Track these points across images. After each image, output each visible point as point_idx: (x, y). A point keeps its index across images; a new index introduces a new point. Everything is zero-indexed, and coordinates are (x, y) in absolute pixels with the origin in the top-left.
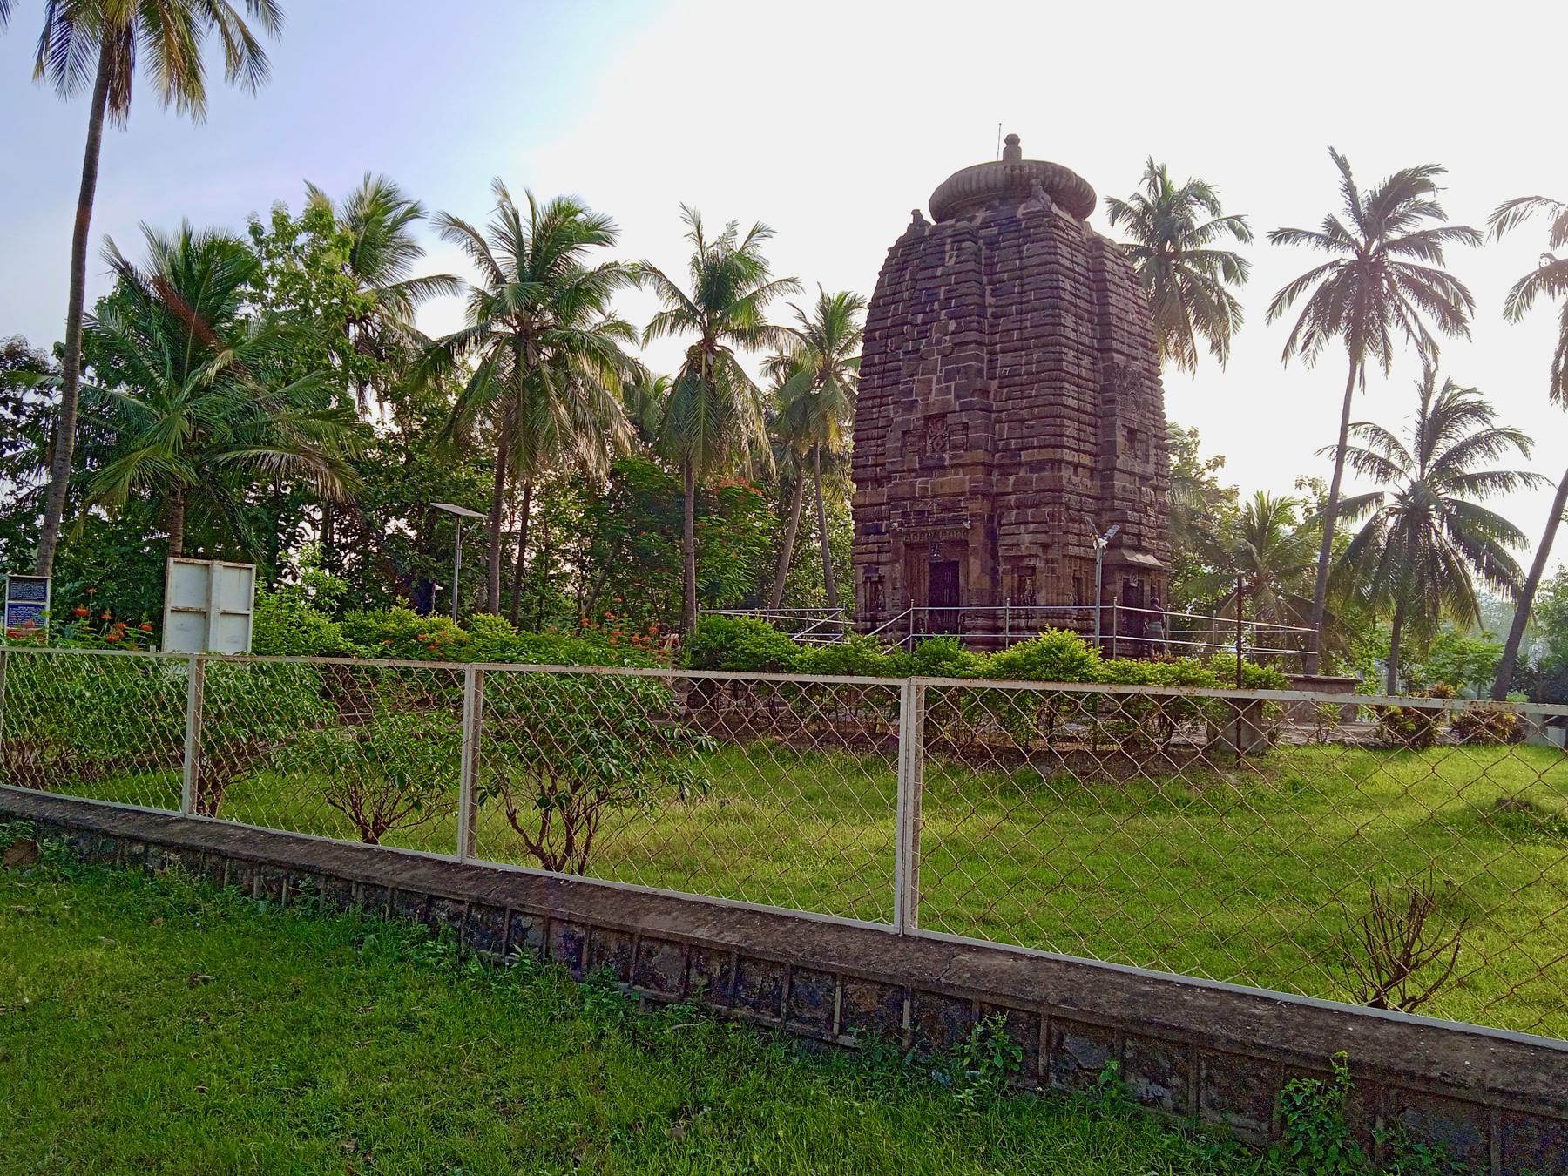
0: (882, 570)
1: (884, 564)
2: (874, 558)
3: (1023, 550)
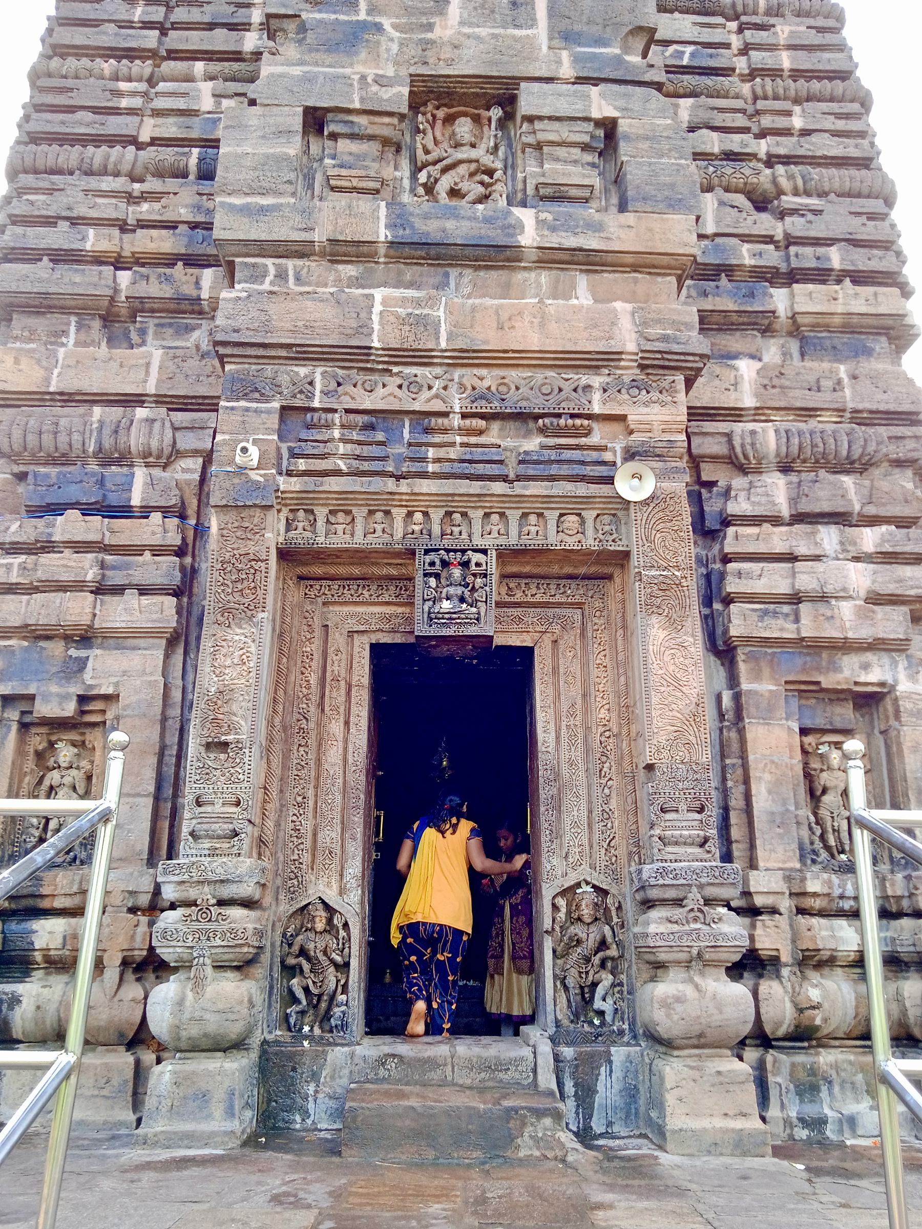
0: (103, 669)
1: (119, 639)
2: (77, 609)
3: (847, 619)
